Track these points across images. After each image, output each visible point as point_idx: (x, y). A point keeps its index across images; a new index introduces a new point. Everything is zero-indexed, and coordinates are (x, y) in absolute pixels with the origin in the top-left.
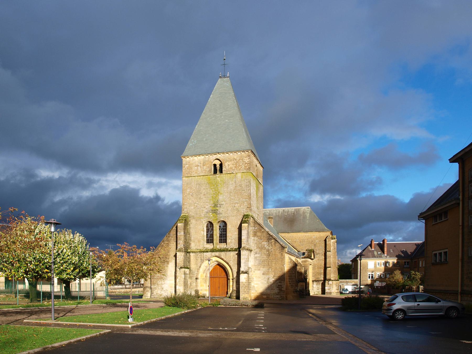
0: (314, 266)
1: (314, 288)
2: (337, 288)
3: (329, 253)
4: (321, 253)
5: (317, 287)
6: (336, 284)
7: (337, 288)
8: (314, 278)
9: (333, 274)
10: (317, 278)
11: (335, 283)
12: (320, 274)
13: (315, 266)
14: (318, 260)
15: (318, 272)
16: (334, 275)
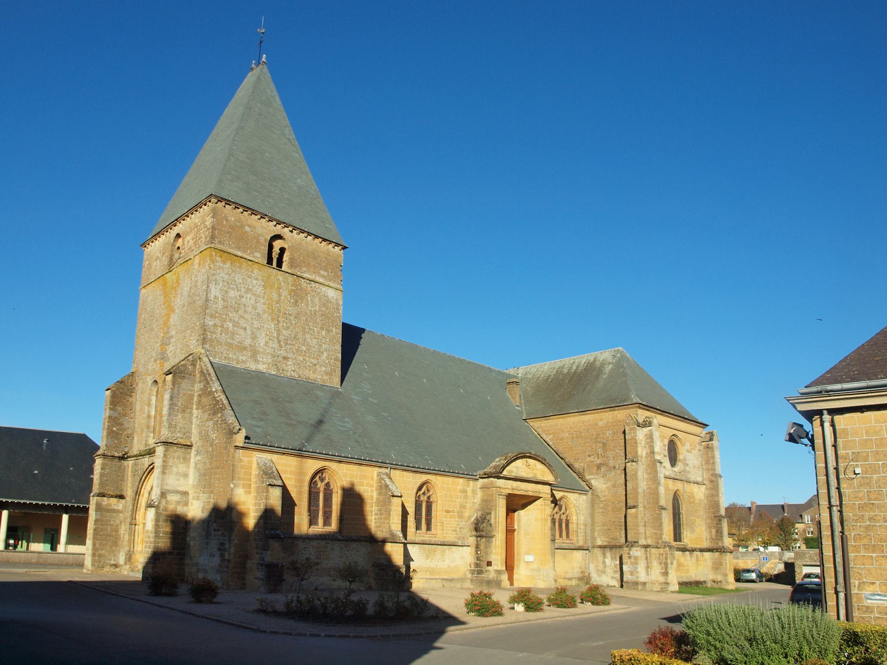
0: (605, 503)
1: (607, 569)
2: (663, 569)
3: (632, 465)
4: (619, 468)
5: (613, 564)
6: (659, 559)
7: (663, 571)
8: (606, 540)
9: (651, 527)
10: (612, 539)
11: (657, 556)
12: (619, 526)
13: (606, 505)
14: (614, 486)
15: (615, 522)
16: (654, 531)
